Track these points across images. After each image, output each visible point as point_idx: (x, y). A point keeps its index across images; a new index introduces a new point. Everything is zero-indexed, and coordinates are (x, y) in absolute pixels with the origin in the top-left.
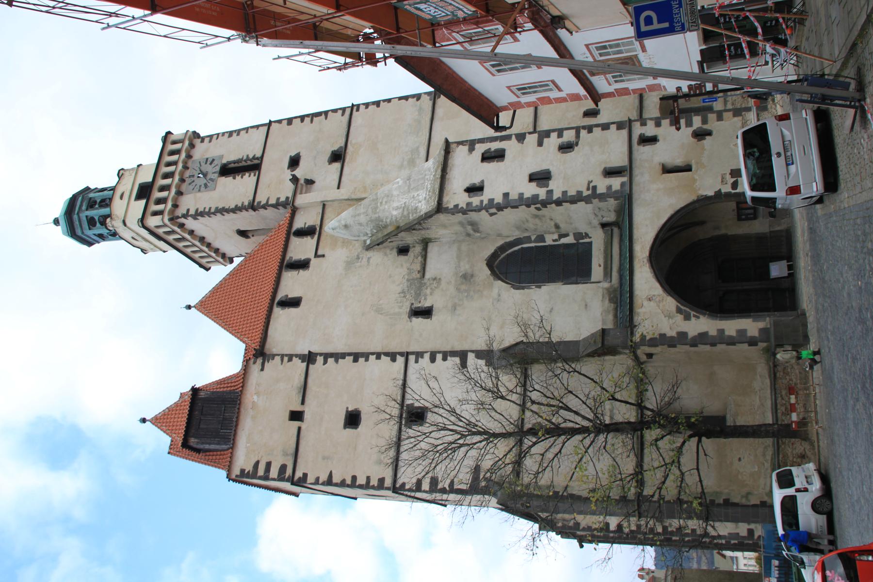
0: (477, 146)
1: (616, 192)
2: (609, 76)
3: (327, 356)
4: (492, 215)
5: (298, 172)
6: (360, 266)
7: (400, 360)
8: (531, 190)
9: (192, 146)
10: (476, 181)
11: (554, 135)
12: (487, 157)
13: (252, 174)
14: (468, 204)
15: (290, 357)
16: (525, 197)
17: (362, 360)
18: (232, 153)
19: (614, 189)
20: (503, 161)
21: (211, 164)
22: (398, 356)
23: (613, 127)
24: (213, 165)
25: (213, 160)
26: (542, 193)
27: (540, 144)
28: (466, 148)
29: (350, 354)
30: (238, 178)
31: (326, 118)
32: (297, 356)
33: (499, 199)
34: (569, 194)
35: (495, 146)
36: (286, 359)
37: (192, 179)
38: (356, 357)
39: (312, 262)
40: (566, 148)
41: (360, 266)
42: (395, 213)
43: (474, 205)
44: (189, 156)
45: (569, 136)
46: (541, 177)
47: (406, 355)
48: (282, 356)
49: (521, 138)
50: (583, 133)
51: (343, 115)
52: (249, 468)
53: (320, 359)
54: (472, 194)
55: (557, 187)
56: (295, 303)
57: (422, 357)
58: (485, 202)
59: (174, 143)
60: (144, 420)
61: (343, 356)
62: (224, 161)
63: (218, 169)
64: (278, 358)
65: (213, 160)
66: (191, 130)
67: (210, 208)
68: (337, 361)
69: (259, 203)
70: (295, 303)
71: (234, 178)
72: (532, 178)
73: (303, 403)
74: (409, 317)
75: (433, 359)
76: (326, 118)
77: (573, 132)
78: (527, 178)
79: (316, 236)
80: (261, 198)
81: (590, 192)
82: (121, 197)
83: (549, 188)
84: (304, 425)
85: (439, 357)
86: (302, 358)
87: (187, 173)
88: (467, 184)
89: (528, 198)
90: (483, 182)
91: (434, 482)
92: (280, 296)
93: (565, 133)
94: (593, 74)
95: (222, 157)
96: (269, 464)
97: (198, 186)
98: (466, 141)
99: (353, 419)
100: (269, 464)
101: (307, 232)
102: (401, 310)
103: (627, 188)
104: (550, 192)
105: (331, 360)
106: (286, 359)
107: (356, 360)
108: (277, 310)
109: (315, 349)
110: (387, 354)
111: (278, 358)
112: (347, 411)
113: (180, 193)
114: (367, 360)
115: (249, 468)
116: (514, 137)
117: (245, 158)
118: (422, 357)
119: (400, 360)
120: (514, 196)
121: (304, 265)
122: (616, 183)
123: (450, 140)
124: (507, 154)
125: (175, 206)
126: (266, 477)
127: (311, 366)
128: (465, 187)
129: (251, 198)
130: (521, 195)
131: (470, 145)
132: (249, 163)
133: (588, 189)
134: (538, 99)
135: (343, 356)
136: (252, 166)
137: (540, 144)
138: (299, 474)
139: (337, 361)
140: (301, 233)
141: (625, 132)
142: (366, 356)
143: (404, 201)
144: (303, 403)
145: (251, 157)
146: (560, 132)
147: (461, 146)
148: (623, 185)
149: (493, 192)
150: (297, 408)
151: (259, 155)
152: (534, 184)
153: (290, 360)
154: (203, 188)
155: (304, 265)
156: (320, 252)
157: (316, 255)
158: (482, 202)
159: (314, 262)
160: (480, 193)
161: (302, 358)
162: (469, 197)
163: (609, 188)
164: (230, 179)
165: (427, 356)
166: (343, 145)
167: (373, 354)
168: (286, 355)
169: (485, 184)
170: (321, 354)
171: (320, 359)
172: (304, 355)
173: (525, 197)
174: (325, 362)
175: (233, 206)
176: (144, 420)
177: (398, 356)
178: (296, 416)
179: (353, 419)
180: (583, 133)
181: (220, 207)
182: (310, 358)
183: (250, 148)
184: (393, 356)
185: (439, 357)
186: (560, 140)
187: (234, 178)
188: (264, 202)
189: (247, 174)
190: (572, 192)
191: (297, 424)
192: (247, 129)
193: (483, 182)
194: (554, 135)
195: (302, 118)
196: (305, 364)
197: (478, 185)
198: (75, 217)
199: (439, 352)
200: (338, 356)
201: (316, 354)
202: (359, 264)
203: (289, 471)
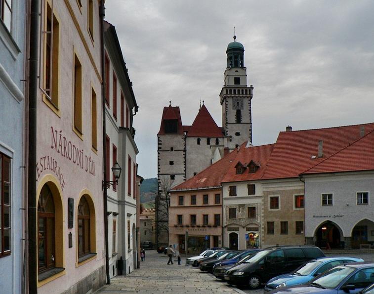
3: (185, 155)
7: (184, 173)
9: (248, 97)
18: (244, 113)
30: (235, 117)
38: (185, 162)
44: (244, 97)
47: (185, 174)
52: (160, 139)
53: (184, 153)
56: (199, 143)
59: (250, 91)
60: (170, 102)
61: (185, 159)
63: (239, 109)
66: (253, 96)
70: (199, 143)
73: (175, 150)
82: (237, 71)
86: (185, 148)
87: (239, 98)
91: (160, 183)
92: (201, 138)
95: (243, 109)
96: (161, 144)
99: (171, 163)
100: (161, 144)
101: (217, 142)
105: (184, 156)
108: (197, 138)
109: (187, 151)
113: (233, 97)
115: (160, 139)
121: (208, 143)
125: (229, 97)
126: (159, 144)
129: (229, 122)
135: (185, 159)
138: (160, 152)
144: (175, 150)
155: (208, 143)
157: (211, 146)
159: (209, 146)
161: (185, 148)
164: (235, 114)
171: (184, 153)
175: (227, 117)
176: (170, 102)
178: (172, 149)
179: (171, 163)
182: (185, 150)
183: (244, 119)
184: (185, 171)
191: (170, 149)
192: (251, 116)
195: (251, 134)
198: (232, 52)
200: (185, 158)
203: (160, 149)
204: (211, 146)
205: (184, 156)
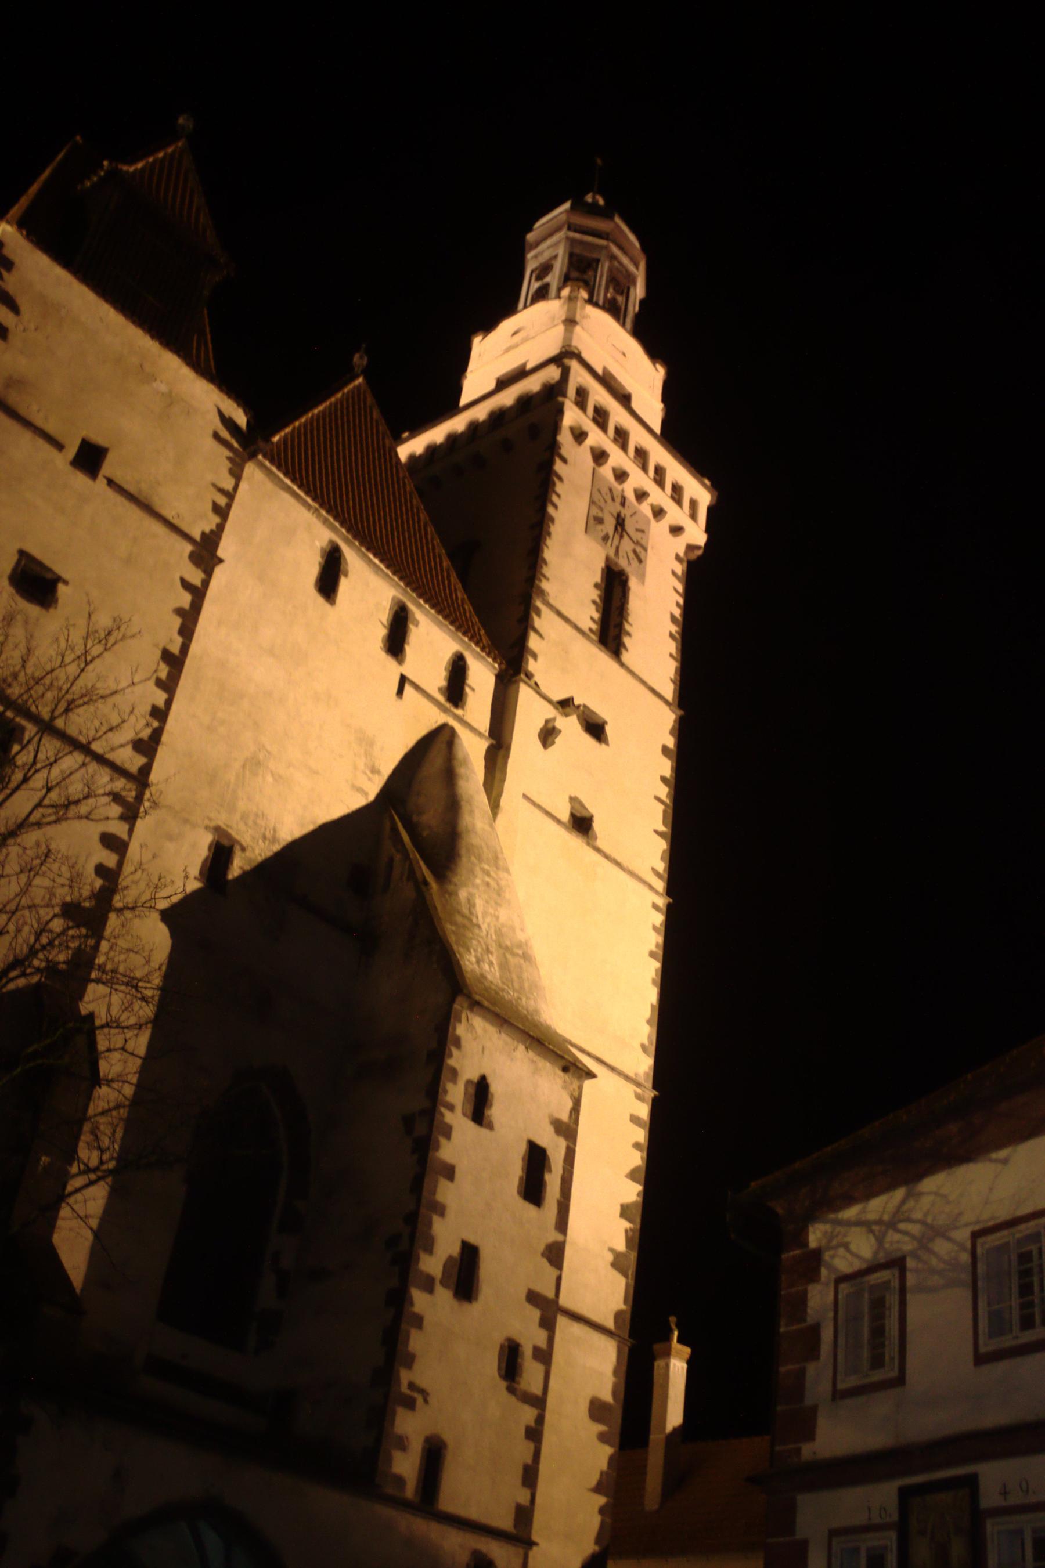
0: (562, 1143)
1: (389, 1460)
2: (891, 1538)
3: (198, 594)
4: (408, 1122)
5: (570, 726)
6: (355, 768)
7: (133, 761)
8: (446, 1238)
10: (496, 1112)
11: (540, 1338)
12: (536, 1158)
13: (594, 627)
14: (454, 1073)
15: (222, 512)
16: (436, 1219)
17: (164, 672)
19: (398, 1456)
20: (519, 1193)
21: (635, 551)
22: (141, 760)
23: (523, 1497)
24: (631, 555)
25: (640, 561)
26: (432, 1264)
27: (533, 1298)
28: (564, 1117)
29: (185, 648)
30: (595, 594)
31: (656, 832)
32: (221, 527)
33: (446, 1152)
34: (414, 1333)
35: (553, 1181)
36: (222, 501)
37: (618, 500)
38: (174, 663)
39: (390, 662)
40: (511, 1360)
41: (355, 768)
42: (463, 894)
43: (450, 1086)
45: (531, 1375)
46: (465, 1275)
48: (230, 496)
49: (555, 1254)
50: (529, 1414)
51: (653, 869)
53: (196, 577)
54: (472, 1090)
55: (434, 1305)
57: (122, 818)
58: (449, 1117)
61: (187, 632)
62: (633, 583)
63: (623, 563)
64: (228, 484)
65: (640, 561)
67: (556, 507)
68: (179, 612)
69: (539, 613)
71: (596, 586)
72: (470, 1254)
74: (217, 830)
75: (109, 841)
76: (656, 832)
77: (536, 1389)
78: (472, 1239)
79: (441, 699)
80: (545, 622)
81: (404, 1388)
83: (439, 1289)
84: (61, 461)
85: (110, 859)
88: (496, 1088)
89: (430, 1224)
90: (490, 1127)
93: (538, 1369)
94: (904, 1494)
95: (642, 578)
97: (602, 503)
98: (576, 1122)
102: (237, 816)
103: (390, 1490)
104: (428, 1285)
105: (185, 599)
106: (222, 501)
107: (166, 656)
110: (156, 736)
111: (228, 484)
112: (58, 579)
114: (159, 683)
116: (560, 1237)
117: (627, 627)
118: (122, 818)
119: (133, 761)
120: (446, 1192)
121: (396, 642)
122: (406, 1466)
123: (588, 1084)
124: (530, 1209)
127: (188, 548)
128: (490, 1080)
129: (552, 601)
130: (440, 1210)
131: (568, 1126)
132: (613, 632)
133: (412, 1386)
134: (815, 1330)
136: (611, 634)
137: (533, 1298)
139: (179, 612)
140: (458, 671)
141: (506, 1522)
142: (169, 686)
143: (484, 927)
145: (626, 640)
146: (544, 1356)
147: (569, 1104)
148: (400, 1481)
149: (461, 1142)
150: (108, 468)
151: (625, 657)
152: (455, 1250)
153: (216, 509)
154: (595, 511)
155: (396, 642)
156: (408, 689)
158: (451, 1108)
159: (392, 669)
160: (469, 1112)
162: (469, 1082)
163: (402, 1444)
164: (598, 578)
165: (119, 829)
166: (600, 843)
167: (169, 703)
168: (229, 506)
169: (483, 1132)
170: (206, 583)
171: (196, 577)
172: (216, 545)
173: (436, 1219)
174: (186, 585)
175: (547, 554)
177: (141, 760)
180: (529, 1414)
181: (553, 529)
182: (206, 553)
185: (110, 859)
186: (527, 1351)
187: (596, 586)
188: (537, 622)
189: (597, 616)
190: (416, 1342)
193: (490, 1127)
194: (540, 1338)
196: (197, 537)
197: (487, 1112)
199: (120, 864)
201: (209, 574)
202: (362, 766)
204: (403, 680)
205: (185, 599)
